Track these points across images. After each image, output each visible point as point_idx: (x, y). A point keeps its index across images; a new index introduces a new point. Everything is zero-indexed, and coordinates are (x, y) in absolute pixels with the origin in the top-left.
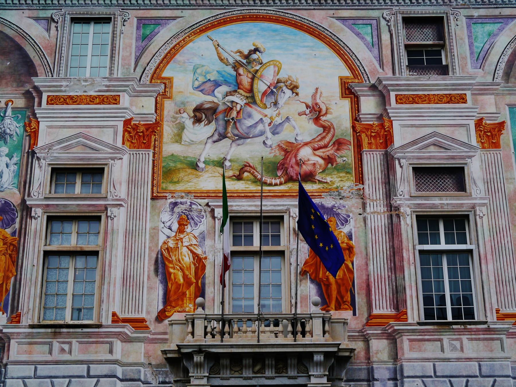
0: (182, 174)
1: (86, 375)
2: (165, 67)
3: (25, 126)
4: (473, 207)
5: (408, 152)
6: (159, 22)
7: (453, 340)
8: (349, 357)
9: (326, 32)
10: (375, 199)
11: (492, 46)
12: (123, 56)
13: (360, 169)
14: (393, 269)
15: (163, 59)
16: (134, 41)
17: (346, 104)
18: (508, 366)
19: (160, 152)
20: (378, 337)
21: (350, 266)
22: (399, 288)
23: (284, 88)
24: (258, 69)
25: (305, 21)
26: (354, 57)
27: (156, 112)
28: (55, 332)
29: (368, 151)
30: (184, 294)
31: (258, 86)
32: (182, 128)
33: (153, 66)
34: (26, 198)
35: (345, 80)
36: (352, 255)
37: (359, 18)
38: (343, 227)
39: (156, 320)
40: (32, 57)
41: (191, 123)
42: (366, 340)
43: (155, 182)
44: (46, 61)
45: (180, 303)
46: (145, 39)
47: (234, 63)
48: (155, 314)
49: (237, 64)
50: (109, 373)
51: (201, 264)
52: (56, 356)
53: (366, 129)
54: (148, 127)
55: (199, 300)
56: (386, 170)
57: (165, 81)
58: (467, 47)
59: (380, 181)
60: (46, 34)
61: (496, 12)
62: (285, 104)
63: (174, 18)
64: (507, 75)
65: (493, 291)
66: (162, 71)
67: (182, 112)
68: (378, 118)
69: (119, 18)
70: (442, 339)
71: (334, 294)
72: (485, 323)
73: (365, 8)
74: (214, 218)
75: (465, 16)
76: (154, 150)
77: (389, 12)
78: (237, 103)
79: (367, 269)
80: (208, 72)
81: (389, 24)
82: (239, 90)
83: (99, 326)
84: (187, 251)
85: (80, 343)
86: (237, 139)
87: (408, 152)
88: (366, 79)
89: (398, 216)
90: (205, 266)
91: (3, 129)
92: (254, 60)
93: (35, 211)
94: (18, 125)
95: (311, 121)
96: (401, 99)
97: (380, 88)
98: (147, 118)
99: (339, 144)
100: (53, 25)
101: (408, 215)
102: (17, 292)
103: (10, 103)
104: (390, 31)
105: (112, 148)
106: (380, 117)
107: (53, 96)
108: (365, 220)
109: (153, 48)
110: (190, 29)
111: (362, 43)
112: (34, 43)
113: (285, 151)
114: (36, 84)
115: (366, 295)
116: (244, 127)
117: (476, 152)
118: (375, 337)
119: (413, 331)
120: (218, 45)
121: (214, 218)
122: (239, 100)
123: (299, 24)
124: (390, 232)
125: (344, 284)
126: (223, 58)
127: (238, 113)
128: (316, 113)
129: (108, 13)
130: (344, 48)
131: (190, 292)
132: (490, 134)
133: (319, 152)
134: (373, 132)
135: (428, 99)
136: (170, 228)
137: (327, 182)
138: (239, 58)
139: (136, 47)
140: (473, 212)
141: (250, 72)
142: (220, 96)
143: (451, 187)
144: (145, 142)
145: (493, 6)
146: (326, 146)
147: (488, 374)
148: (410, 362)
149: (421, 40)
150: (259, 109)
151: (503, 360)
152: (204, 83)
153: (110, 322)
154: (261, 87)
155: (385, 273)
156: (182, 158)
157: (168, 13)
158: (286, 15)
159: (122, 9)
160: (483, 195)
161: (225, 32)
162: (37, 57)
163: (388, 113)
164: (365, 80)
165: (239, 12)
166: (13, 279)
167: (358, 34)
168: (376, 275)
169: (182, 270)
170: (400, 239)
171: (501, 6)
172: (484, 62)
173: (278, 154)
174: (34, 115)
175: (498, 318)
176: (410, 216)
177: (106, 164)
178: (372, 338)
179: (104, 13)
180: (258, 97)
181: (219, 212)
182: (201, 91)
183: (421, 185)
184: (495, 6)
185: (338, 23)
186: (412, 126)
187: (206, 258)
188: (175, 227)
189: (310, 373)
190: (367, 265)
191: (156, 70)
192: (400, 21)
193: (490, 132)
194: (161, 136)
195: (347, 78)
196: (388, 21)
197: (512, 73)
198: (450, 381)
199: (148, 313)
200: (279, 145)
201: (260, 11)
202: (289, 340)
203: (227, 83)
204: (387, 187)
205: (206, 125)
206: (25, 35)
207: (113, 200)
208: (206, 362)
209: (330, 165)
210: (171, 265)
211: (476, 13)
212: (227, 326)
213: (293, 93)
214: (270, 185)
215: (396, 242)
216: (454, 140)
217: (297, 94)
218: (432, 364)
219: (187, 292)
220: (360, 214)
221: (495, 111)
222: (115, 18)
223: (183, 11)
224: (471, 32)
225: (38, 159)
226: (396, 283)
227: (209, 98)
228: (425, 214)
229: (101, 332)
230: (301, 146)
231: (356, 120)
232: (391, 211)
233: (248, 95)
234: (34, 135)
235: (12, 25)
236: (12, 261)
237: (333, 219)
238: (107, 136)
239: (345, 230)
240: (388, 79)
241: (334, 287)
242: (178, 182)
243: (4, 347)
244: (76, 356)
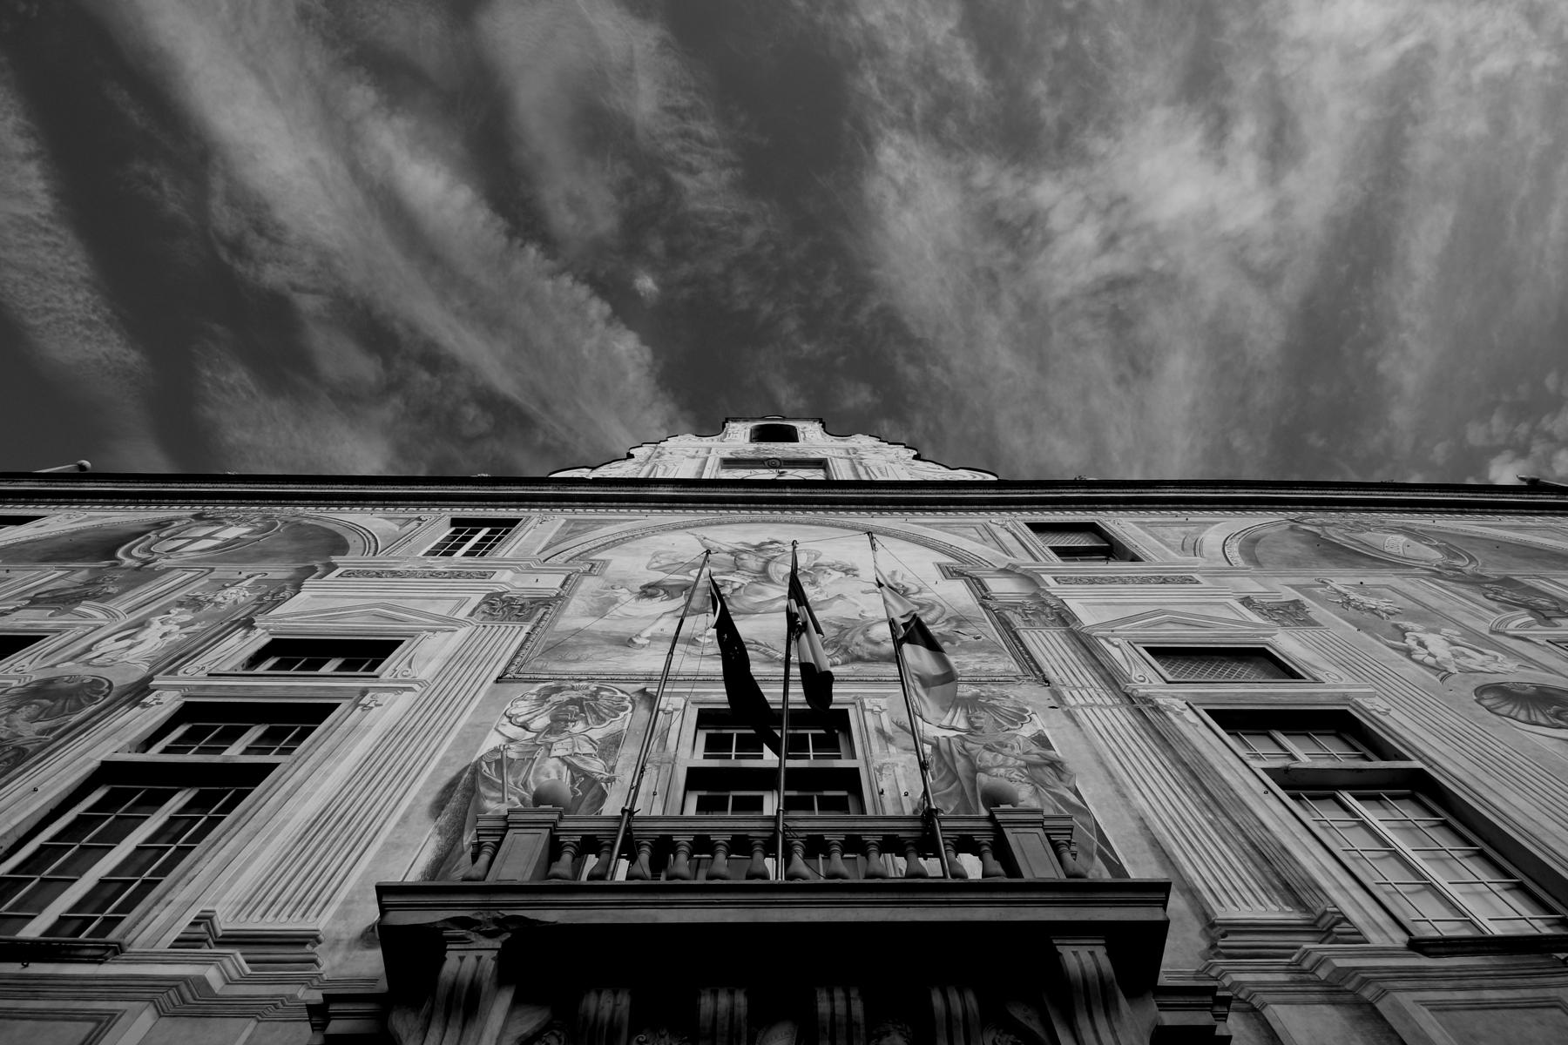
0: (589, 652)
36: (1064, 777)
39: (362, 936)
51: (594, 790)
79: (1128, 805)
108: (1071, 716)
155: (1195, 816)
215: (1181, 752)
216: (1209, 618)
239: (1027, 731)
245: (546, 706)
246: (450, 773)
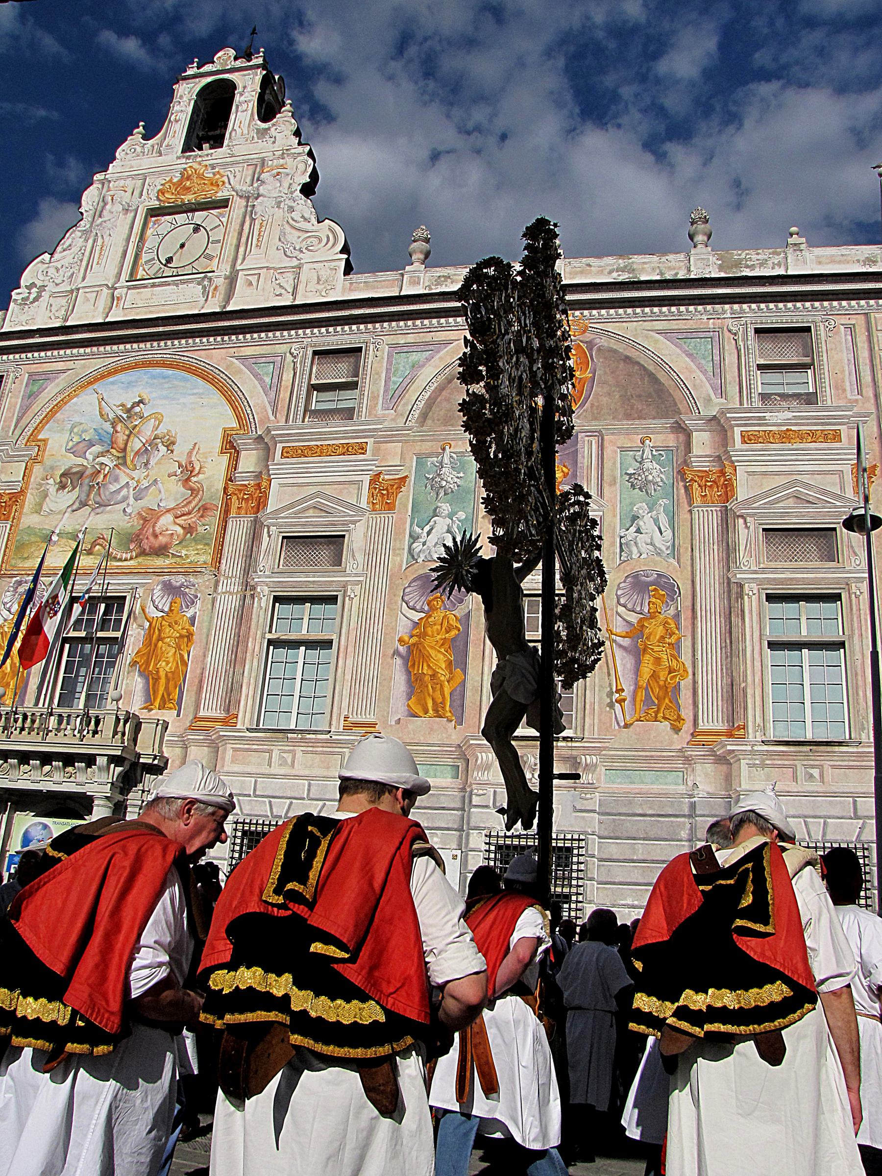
4: (345, 586)
24: (137, 423)
32: (45, 495)
37: (262, 356)
46: (31, 396)
53: (239, 490)
56: (251, 540)
57: (39, 443)
61: (428, 337)
64: (424, 416)
65: (346, 693)
66: (39, 432)
70: (272, 750)
79: (203, 661)
80: (86, 431)
89: (253, 596)
92: (136, 414)
96: (287, 452)
99: (205, 509)
106: (259, 475)
108: (214, 600)
109: (35, 408)
113: (145, 520)
116: (107, 493)
127: (105, 476)
128: (188, 472)
135: (319, 451)
136: (9, 611)
137: (181, 556)
138: (120, 413)
142: (90, 457)
150: (128, 471)
154: (136, 444)
155: (223, 666)
157: (60, 366)
161: (113, 383)
167: (256, 375)
193: (387, 489)
194: (22, 507)
195: (232, 429)
197: (430, 414)
198: (270, 802)
203: (101, 441)
211: (402, 340)
214: (120, 560)
215: (243, 628)
217: (172, 451)
218: (253, 780)
224: (391, 365)
227: (80, 461)
233: (120, 455)
237: (178, 600)
241: (163, 681)
242: (27, 558)
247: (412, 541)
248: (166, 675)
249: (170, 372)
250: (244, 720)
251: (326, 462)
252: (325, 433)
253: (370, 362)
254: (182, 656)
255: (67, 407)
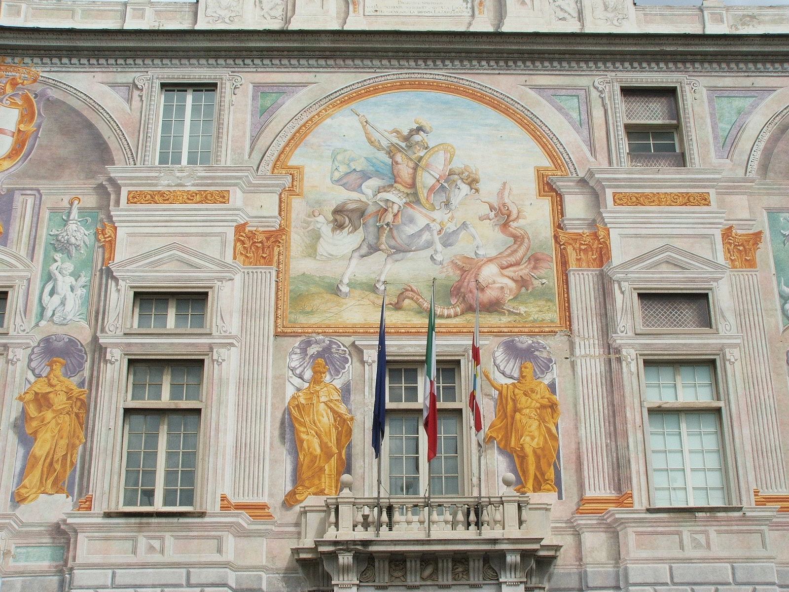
0: (317, 302)
1: (184, 583)
2: (292, 151)
3: (96, 234)
4: (722, 348)
5: (632, 272)
6: (283, 89)
7: (697, 532)
8: (554, 558)
9: (516, 105)
10: (586, 336)
11: (741, 128)
12: (233, 136)
13: (566, 295)
14: (613, 434)
15: (290, 141)
16: (249, 117)
17: (545, 205)
18: (773, 569)
19: (287, 271)
20: (592, 528)
21: (554, 430)
22: (621, 461)
23: (459, 182)
25: (487, 90)
26: (555, 141)
27: (280, 214)
28: (141, 523)
29: (577, 270)
30: (322, 469)
31: (423, 179)
32: (316, 236)
33: (274, 152)
34: (98, 334)
35: (544, 172)
36: (555, 415)
38: (542, 376)
40: (106, 137)
41: (330, 229)
42: (577, 534)
43: (279, 312)
44: (125, 143)
45: (316, 482)
46: (264, 114)
47: (388, 147)
48: (281, 497)
49: (392, 148)
50: (218, 581)
52: (143, 556)
54: (269, 235)
55: (346, 477)
56: (602, 297)
57: (292, 171)
58: (710, 130)
59: (594, 312)
60: (126, 106)
61: (747, 82)
62: (460, 204)
63: (304, 85)
64: (764, 168)
65: (750, 465)
66: (288, 157)
67: (316, 214)
68: (589, 224)
69: (228, 84)
70: (681, 532)
71: (532, 469)
72: (740, 509)
73: (569, 73)
74: (363, 362)
75: (705, 87)
76: (278, 267)
77: (602, 80)
78: (393, 203)
80: (353, 160)
81: (603, 96)
82: (396, 185)
83: (202, 515)
84: (324, 410)
85: (177, 538)
86: (394, 253)
87: (632, 272)
88: (573, 170)
89: (619, 360)
90: (351, 430)
91: (66, 237)
92: (417, 143)
93: (111, 352)
94: (87, 233)
95: (497, 228)
96: (620, 199)
97: (592, 183)
98: (267, 222)
99: (536, 260)
100: (136, 93)
101: (632, 360)
102: (86, 466)
103: (76, 202)
104: (604, 106)
105: (218, 265)
106: (593, 224)
107: (136, 191)
108: (573, 365)
109: (275, 125)
110: (327, 99)
111: (566, 122)
112: (109, 119)
114: (112, 175)
115: (577, 471)
116: (404, 236)
117: (723, 273)
118: (589, 530)
119: (641, 521)
120: (366, 122)
121: (363, 362)
122: (396, 198)
123: (479, 94)
124: (608, 382)
125: (545, 456)
126: (373, 139)
127: (395, 215)
128: (504, 217)
129: (213, 77)
130: (541, 128)
131: (330, 467)
132: (742, 248)
133: (508, 272)
134: (581, 244)
136: (301, 377)
137: (520, 314)
138: (395, 140)
139: (252, 124)
140: (721, 355)
141: (411, 160)
142: (369, 192)
143: (691, 320)
144: (264, 255)
145: (743, 74)
146: (517, 264)
147: (745, 581)
148: (638, 563)
149: (647, 119)
150: (424, 211)
151: (765, 560)
152: (347, 174)
153: (217, 509)
154: (426, 180)
155: (602, 441)
156: (318, 279)
158: (461, 81)
159: (232, 72)
160: (734, 332)
162: (113, 138)
163: (603, 219)
164: (571, 172)
165: (395, 77)
166: (80, 448)
167: (560, 109)
168: (589, 442)
169: (319, 436)
170: (622, 393)
171: (754, 74)
172: (732, 149)
173: (451, 274)
174: (110, 218)
175: (758, 503)
176: (635, 360)
177: (211, 288)
178: (585, 530)
179: (207, 77)
180: (423, 194)
181: (372, 355)
182: (343, 185)
183: (649, 317)
184: (746, 74)
185: (532, 93)
186: (637, 236)
187: (352, 419)
188: (308, 374)
189: (501, 580)
190: (577, 428)
191: (279, 156)
192: (618, 91)
193: (742, 245)
194: (287, 248)
196: (601, 92)
199: (271, 495)
200: (452, 262)
201: (425, 76)
202: (471, 533)
203: (378, 174)
204: (604, 321)
205: (351, 232)
206: (97, 107)
207: (220, 337)
208: (355, 565)
209: (523, 290)
210: (303, 429)
212: (384, 514)
213: (471, 189)
215: (616, 396)
216: (693, 256)
217: (477, 191)
218: (667, 566)
219: (326, 467)
220: (567, 358)
221: (748, 217)
222: (222, 84)
223: (317, 74)
224: (714, 109)
225: (116, 280)
226: (617, 454)
227: (355, 195)
228: (656, 357)
229: (206, 523)
230: (483, 262)
231: (559, 227)
232: (609, 353)
233: (409, 191)
234: (110, 246)
235: (79, 94)
236: (80, 423)
237: (529, 365)
238: (213, 249)
239: (547, 380)
240: (602, 171)
241: (531, 459)
242: (312, 312)
243: (68, 544)
244: (171, 556)
245: (307, 358)
246: (279, 415)
247: (783, 301)
248: (534, 452)
249: (450, 97)
250: (640, 502)
251: (667, 212)
252: (659, 180)
253: (690, 105)
254: (549, 431)
255: (319, 129)
